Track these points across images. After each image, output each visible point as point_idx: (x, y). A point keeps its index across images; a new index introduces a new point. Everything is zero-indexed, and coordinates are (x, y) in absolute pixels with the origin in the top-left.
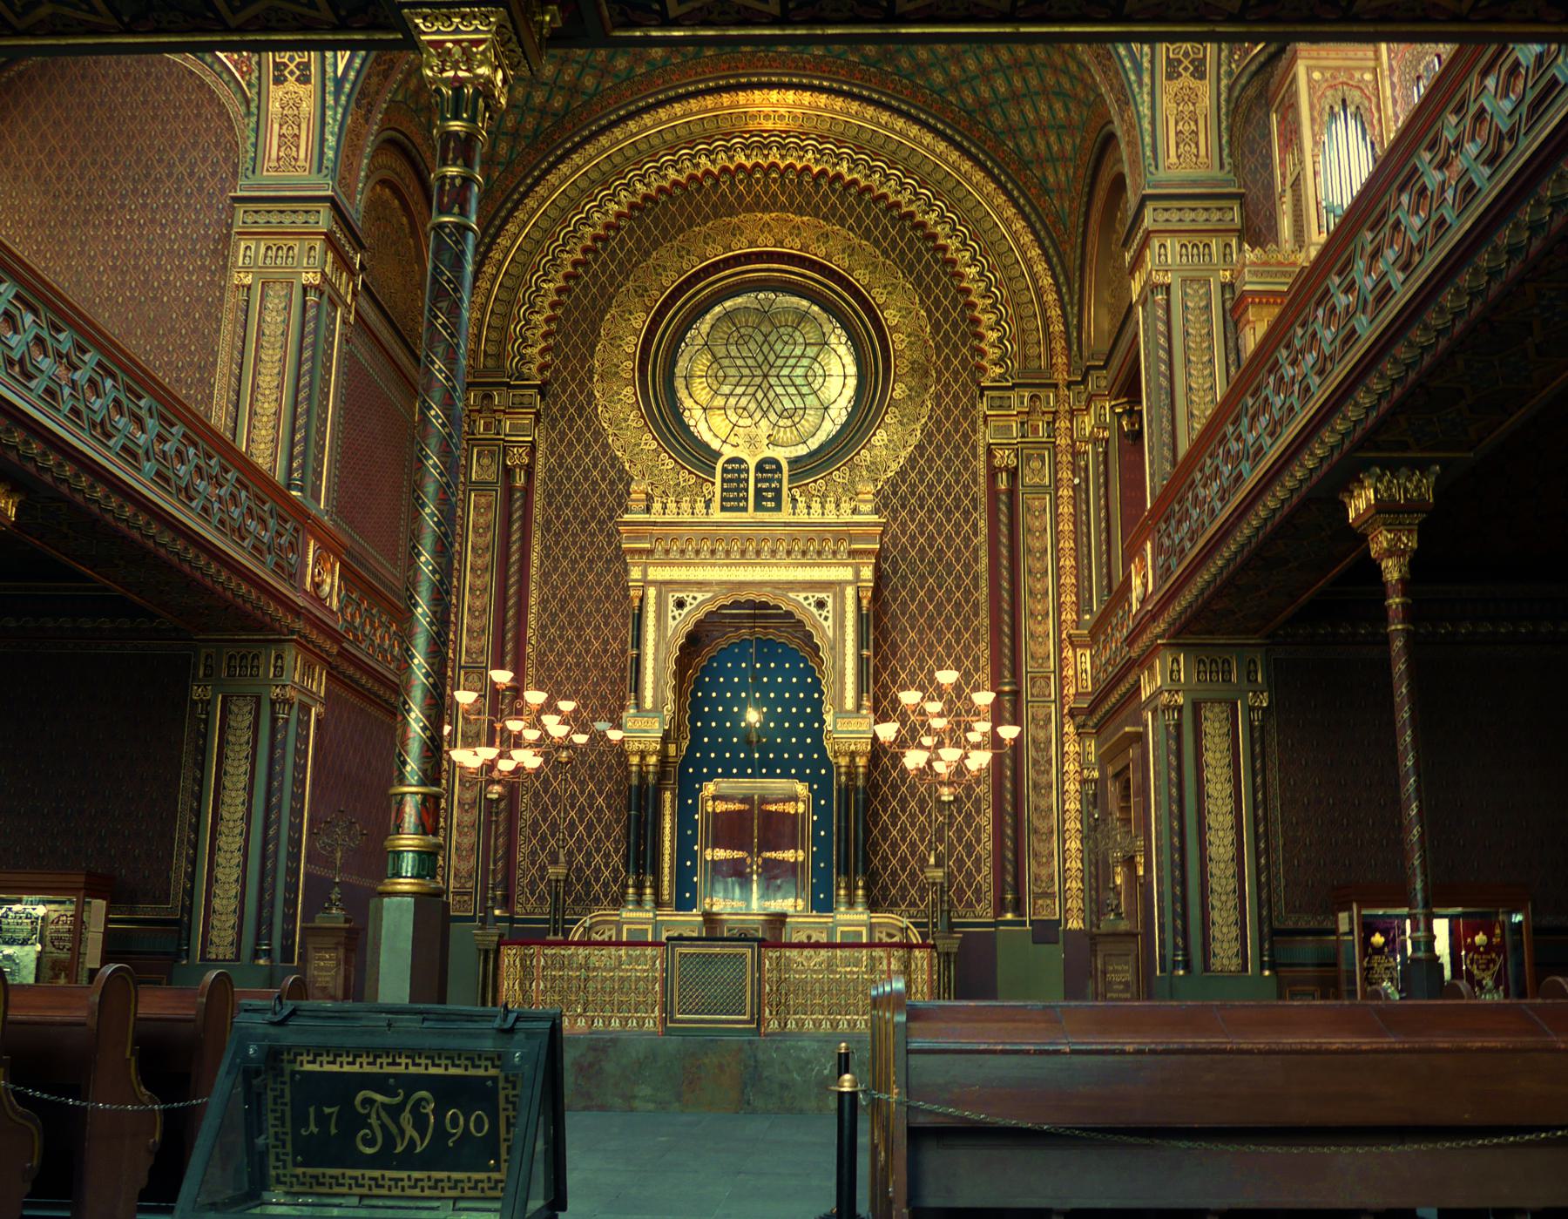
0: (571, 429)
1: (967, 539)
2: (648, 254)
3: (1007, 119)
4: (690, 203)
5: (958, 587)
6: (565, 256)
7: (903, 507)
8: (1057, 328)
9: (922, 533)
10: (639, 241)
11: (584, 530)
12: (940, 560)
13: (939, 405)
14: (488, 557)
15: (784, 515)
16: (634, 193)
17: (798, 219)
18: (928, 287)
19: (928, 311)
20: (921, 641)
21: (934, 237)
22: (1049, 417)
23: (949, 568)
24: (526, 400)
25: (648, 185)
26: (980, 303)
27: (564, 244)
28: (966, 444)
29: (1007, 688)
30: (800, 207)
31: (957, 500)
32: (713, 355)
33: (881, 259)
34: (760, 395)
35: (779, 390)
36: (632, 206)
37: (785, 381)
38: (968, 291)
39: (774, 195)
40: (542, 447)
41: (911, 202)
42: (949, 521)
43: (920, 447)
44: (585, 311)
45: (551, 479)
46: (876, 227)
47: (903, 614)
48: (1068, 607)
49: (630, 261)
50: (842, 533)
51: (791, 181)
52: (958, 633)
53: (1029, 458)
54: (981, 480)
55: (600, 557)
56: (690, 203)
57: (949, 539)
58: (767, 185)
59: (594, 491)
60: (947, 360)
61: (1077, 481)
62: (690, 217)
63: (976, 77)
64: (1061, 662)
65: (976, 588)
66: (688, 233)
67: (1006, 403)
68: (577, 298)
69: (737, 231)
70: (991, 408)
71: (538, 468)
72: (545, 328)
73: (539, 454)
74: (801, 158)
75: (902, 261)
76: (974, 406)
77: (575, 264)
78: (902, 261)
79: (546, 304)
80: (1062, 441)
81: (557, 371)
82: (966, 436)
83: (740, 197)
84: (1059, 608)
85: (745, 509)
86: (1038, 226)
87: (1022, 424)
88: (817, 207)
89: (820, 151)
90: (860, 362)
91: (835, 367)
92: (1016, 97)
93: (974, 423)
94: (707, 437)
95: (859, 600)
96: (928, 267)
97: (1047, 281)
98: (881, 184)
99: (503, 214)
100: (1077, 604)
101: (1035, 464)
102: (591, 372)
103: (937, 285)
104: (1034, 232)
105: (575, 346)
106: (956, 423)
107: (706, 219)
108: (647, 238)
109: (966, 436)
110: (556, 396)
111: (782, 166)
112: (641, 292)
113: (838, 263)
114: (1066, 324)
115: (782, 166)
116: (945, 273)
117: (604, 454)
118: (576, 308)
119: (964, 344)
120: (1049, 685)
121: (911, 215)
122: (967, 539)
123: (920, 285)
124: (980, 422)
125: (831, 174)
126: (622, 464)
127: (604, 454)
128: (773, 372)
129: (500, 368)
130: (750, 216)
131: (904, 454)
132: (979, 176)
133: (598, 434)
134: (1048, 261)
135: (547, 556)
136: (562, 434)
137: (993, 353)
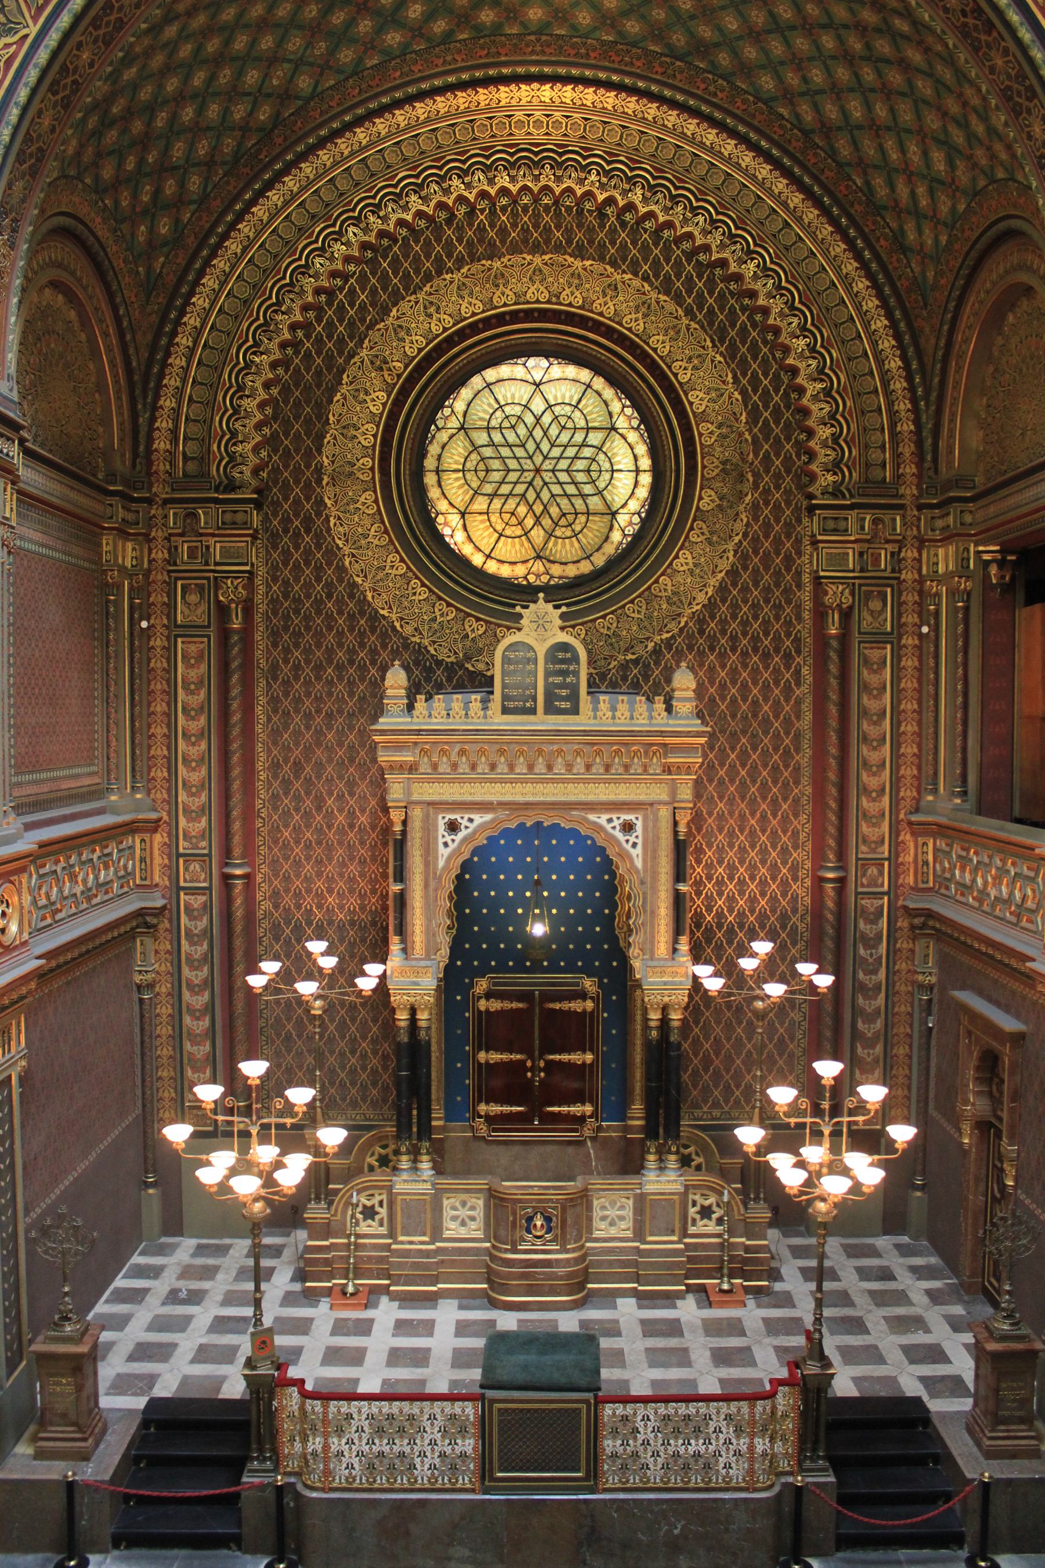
0: (297, 547)
1: (788, 691)
2: (386, 311)
3: (857, 149)
4: (438, 240)
5: (776, 749)
6: (279, 317)
7: (712, 649)
8: (906, 427)
9: (734, 682)
10: (374, 292)
11: (318, 678)
12: (755, 715)
13: (756, 519)
14: (203, 720)
15: (583, 720)
16: (366, 230)
17: (578, 263)
18: (743, 361)
19: (743, 393)
20: (731, 813)
21: (753, 294)
22: (895, 548)
23: (766, 723)
24: (240, 517)
25: (385, 219)
26: (813, 388)
27: (279, 303)
28: (788, 569)
29: (831, 875)
30: (580, 247)
31: (777, 640)
32: (472, 443)
33: (685, 321)
34: (531, 496)
35: (556, 489)
36: (364, 246)
37: (563, 477)
38: (794, 371)
39: (547, 230)
40: (262, 571)
41: (722, 246)
42: (766, 668)
43: (733, 574)
44: (308, 389)
45: (275, 613)
46: (678, 276)
47: (711, 781)
48: (908, 781)
49: (363, 320)
50: (658, 745)
51: (569, 209)
52: (775, 802)
53: (868, 596)
54: (806, 615)
55: (340, 712)
56: (438, 240)
57: (766, 688)
58: (536, 216)
59: (330, 628)
60: (767, 460)
61: (925, 630)
62: (439, 259)
63: (822, 92)
64: (897, 847)
65: (798, 750)
66: (436, 282)
67: (842, 525)
68: (297, 371)
69: (499, 279)
70: (825, 531)
71: (258, 598)
72: (259, 417)
73: (258, 581)
74: (581, 182)
75: (711, 324)
76: (799, 521)
77: (293, 327)
78: (711, 324)
79: (258, 385)
80: (908, 576)
81: (276, 471)
82: (788, 560)
83: (503, 232)
84: (896, 781)
85: (533, 711)
86: (887, 290)
87: (861, 554)
88: (602, 246)
89: (606, 173)
90: (655, 452)
91: (623, 460)
92: (875, 128)
93: (798, 541)
94: (467, 550)
95: (676, 824)
96: (743, 333)
97: (894, 364)
98: (685, 221)
99: (197, 266)
100: (918, 778)
101: (875, 605)
102: (319, 471)
103: (755, 358)
104: (880, 295)
105: (298, 436)
106: (778, 543)
107: (460, 263)
108: (385, 289)
109: (788, 560)
110: (276, 504)
111: (558, 191)
112: (380, 364)
113: (633, 323)
114: (917, 422)
115: (558, 191)
116: (765, 342)
117: (341, 580)
118: (297, 385)
119: (788, 439)
120: (881, 874)
121: (723, 263)
122: (788, 691)
123: (733, 357)
124: (806, 541)
125: (621, 203)
126: (364, 593)
127: (341, 580)
128: (548, 465)
129: (205, 474)
130: (517, 259)
131: (714, 581)
132: (811, 214)
133: (332, 553)
134: (897, 336)
135: (275, 711)
136: (286, 554)
137: (825, 455)
